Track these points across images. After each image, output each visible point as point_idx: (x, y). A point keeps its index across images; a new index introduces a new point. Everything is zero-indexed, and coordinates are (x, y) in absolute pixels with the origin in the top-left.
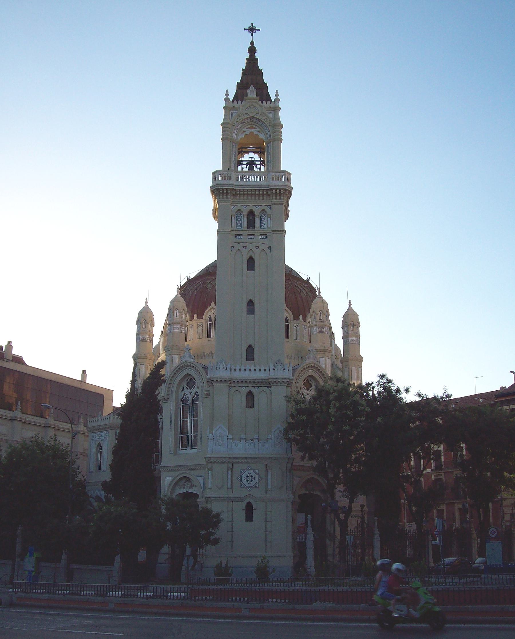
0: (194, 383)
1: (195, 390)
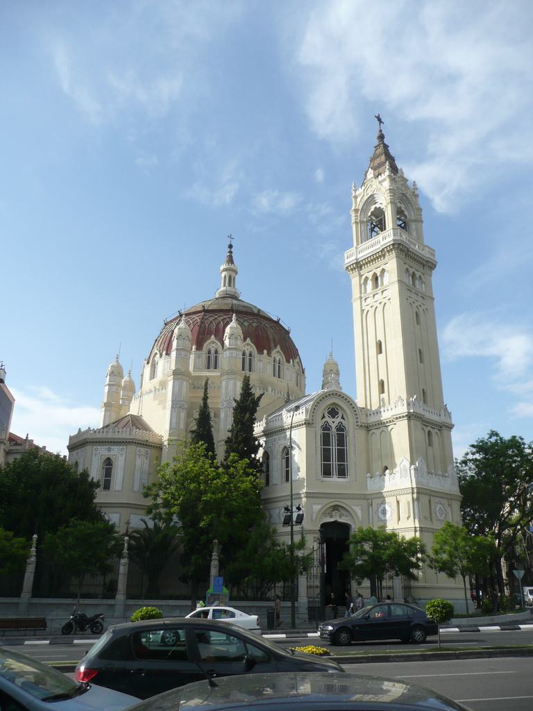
0: (338, 413)
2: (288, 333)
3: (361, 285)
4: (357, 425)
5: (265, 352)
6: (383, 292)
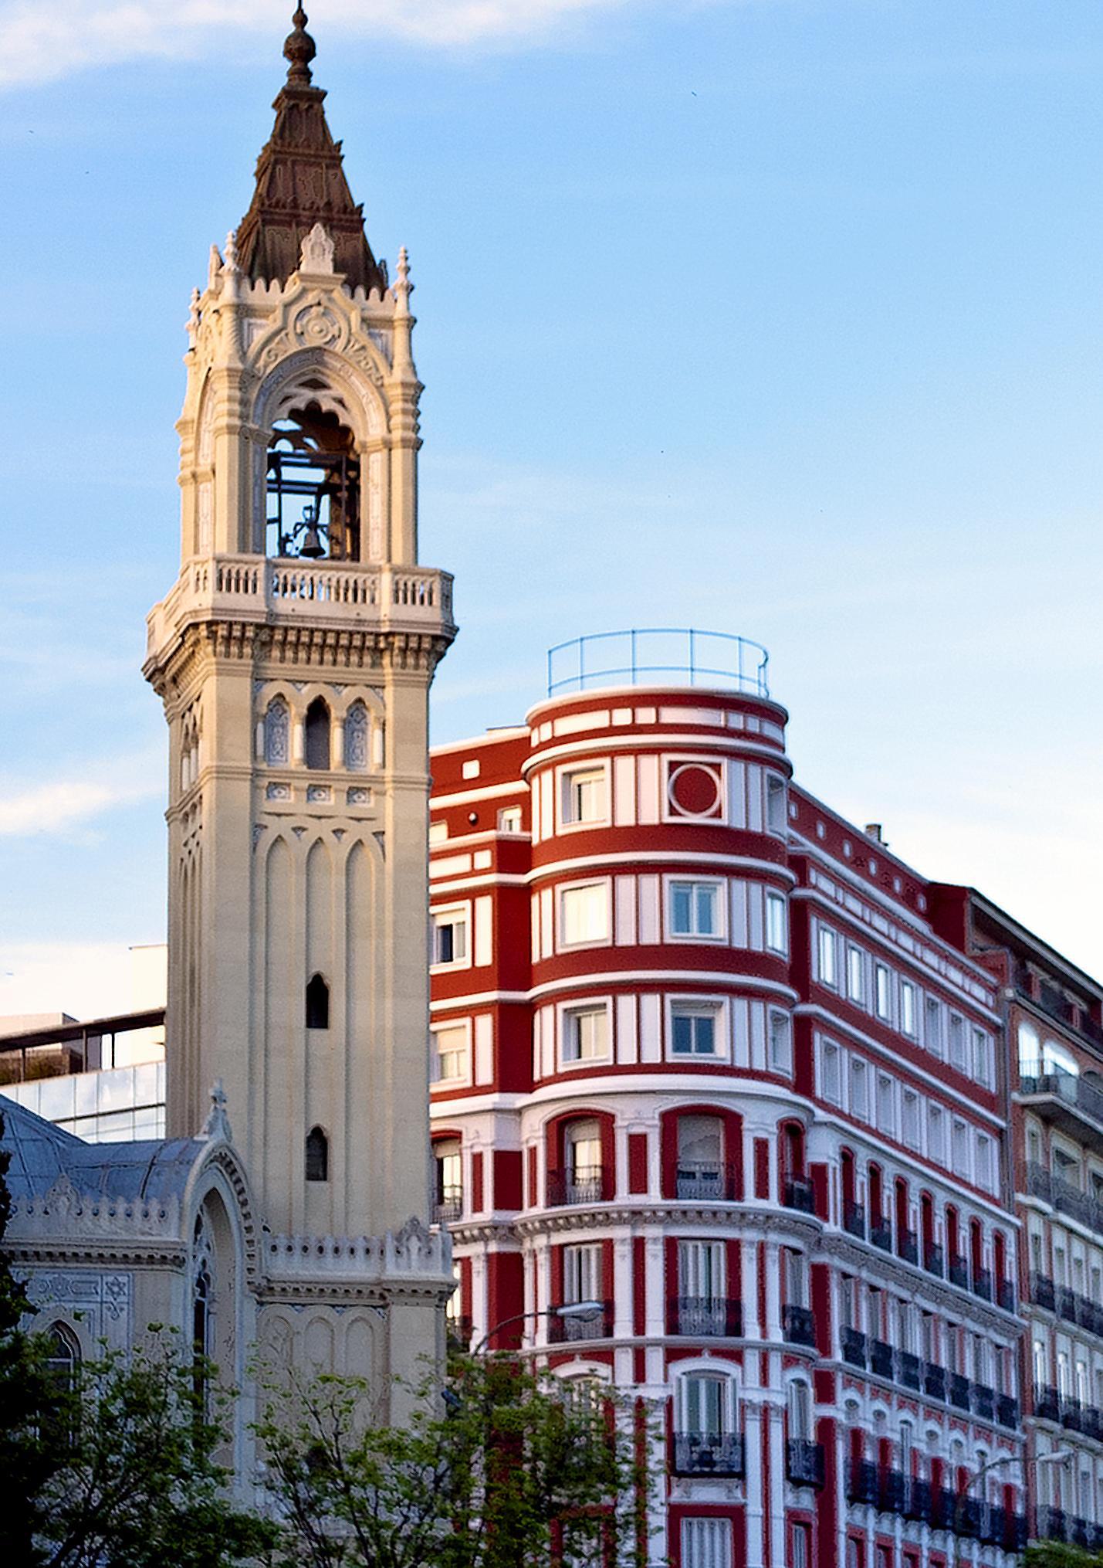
6: (352, 792)
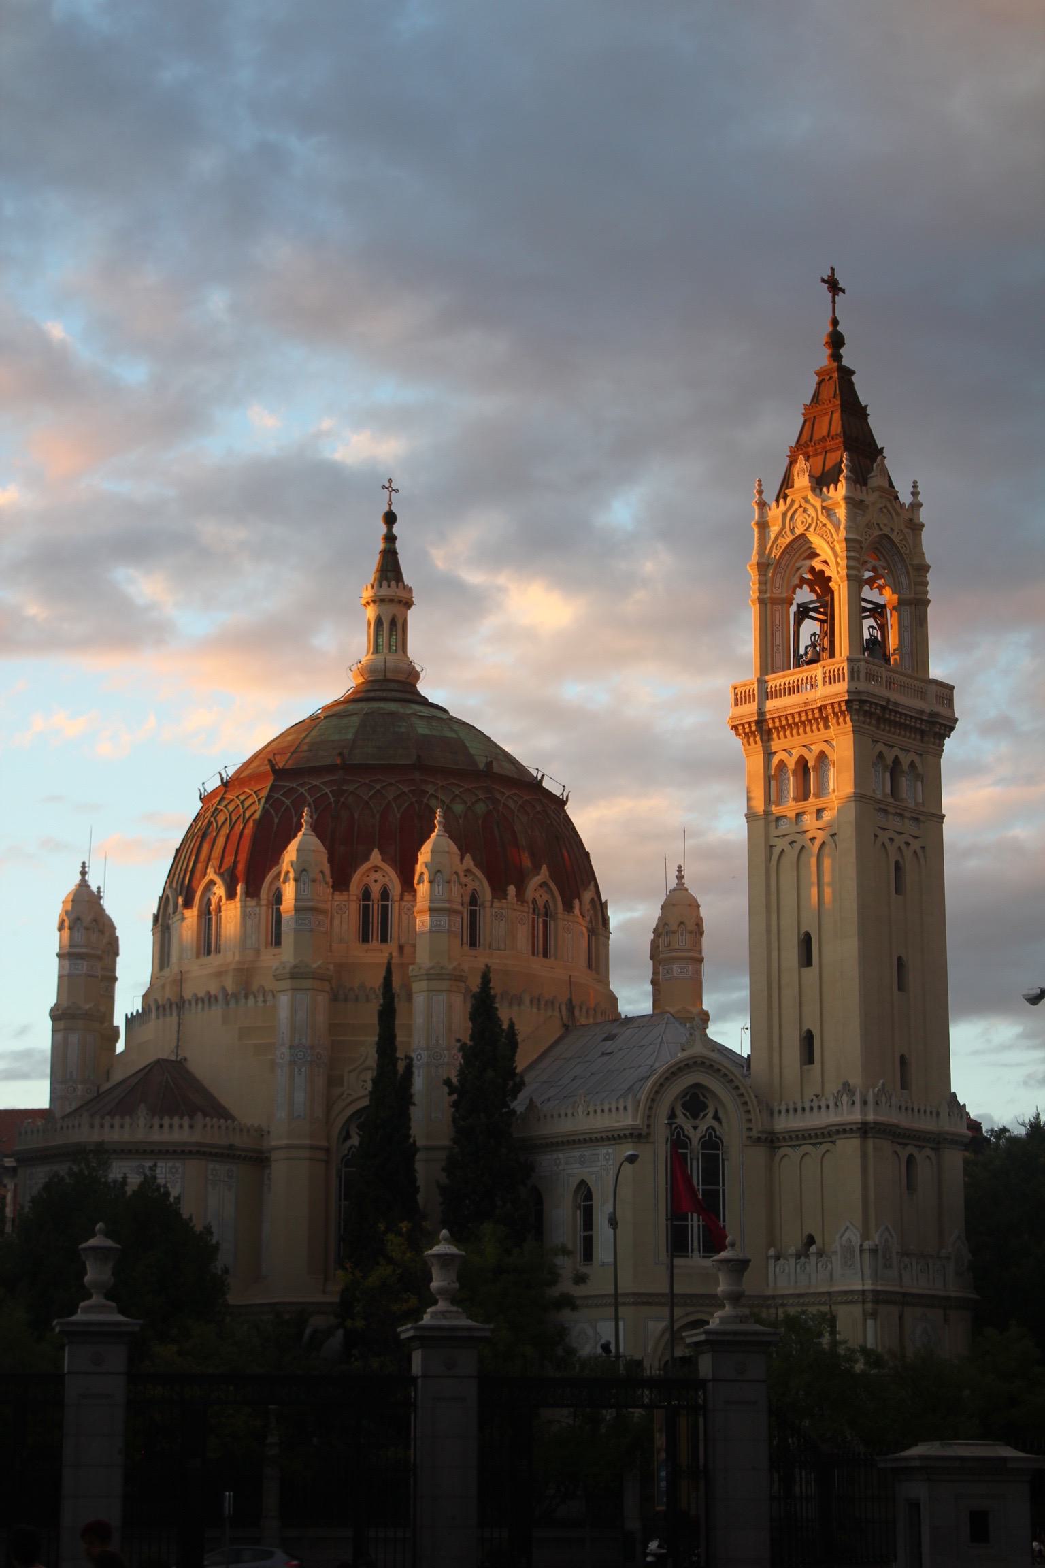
0: (705, 1107)
1: (709, 1121)
2: (561, 803)
3: (768, 779)
4: (749, 1137)
5: (512, 890)
